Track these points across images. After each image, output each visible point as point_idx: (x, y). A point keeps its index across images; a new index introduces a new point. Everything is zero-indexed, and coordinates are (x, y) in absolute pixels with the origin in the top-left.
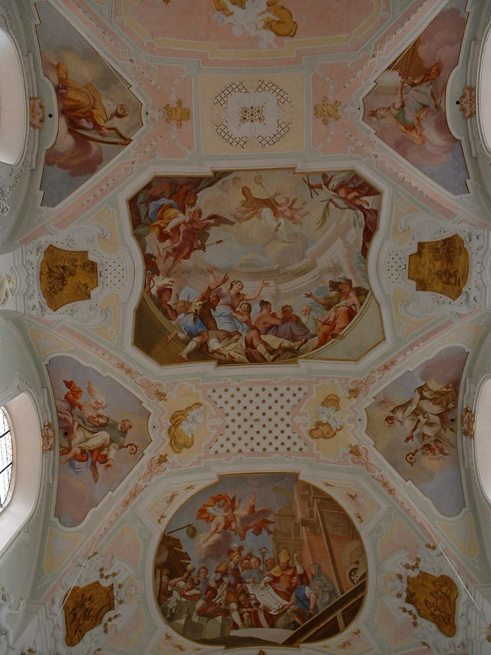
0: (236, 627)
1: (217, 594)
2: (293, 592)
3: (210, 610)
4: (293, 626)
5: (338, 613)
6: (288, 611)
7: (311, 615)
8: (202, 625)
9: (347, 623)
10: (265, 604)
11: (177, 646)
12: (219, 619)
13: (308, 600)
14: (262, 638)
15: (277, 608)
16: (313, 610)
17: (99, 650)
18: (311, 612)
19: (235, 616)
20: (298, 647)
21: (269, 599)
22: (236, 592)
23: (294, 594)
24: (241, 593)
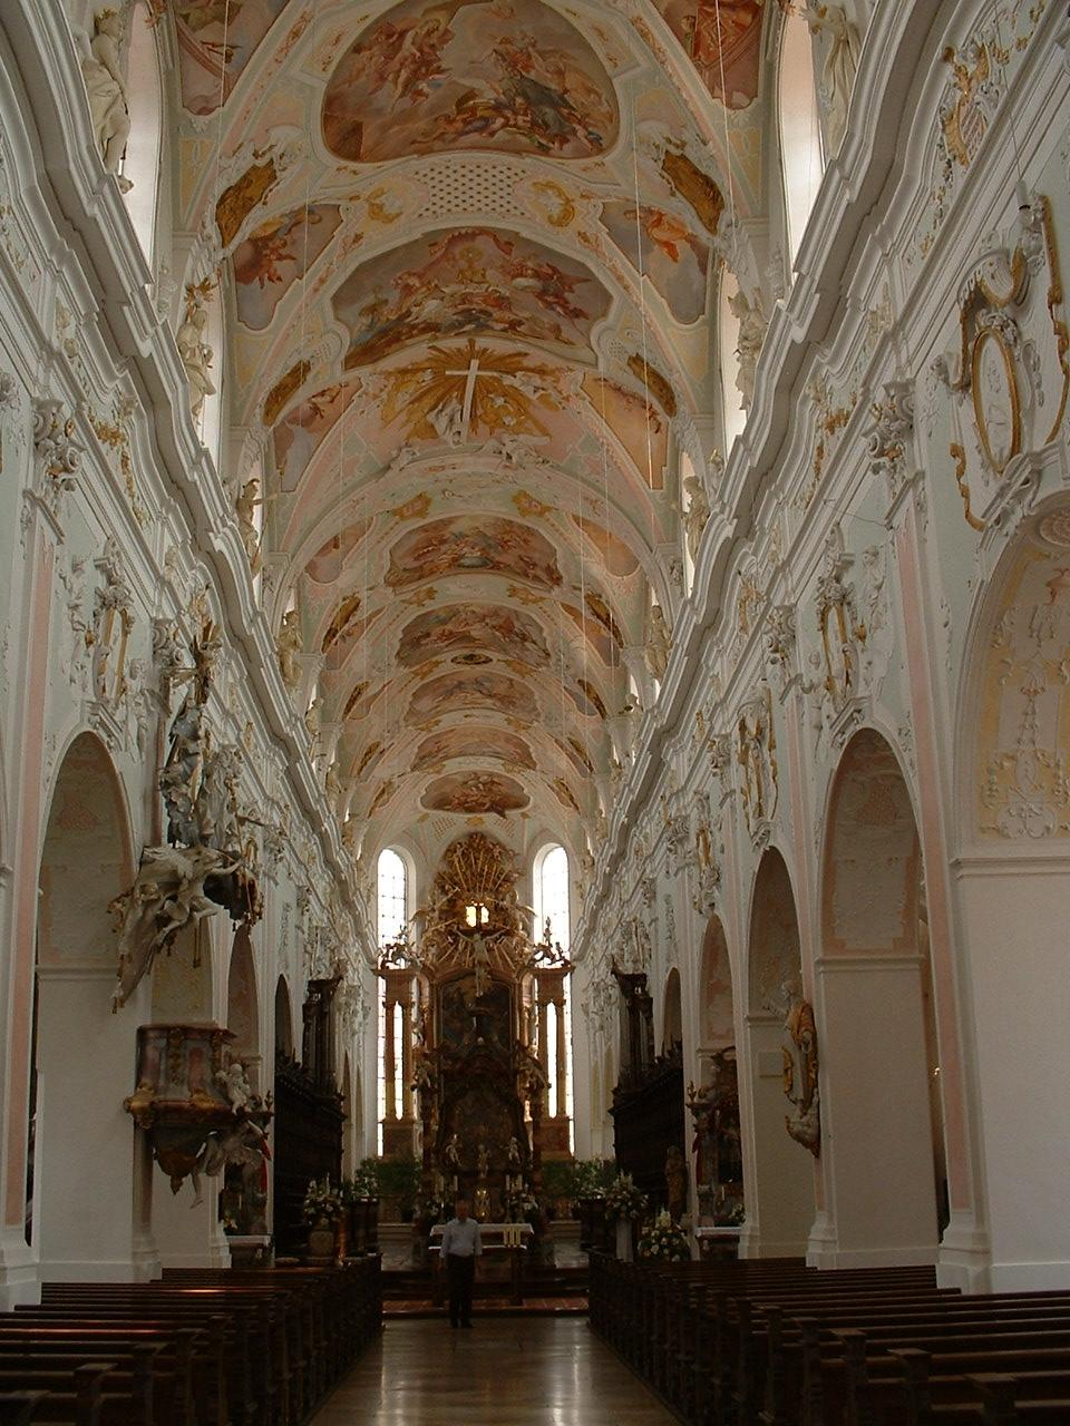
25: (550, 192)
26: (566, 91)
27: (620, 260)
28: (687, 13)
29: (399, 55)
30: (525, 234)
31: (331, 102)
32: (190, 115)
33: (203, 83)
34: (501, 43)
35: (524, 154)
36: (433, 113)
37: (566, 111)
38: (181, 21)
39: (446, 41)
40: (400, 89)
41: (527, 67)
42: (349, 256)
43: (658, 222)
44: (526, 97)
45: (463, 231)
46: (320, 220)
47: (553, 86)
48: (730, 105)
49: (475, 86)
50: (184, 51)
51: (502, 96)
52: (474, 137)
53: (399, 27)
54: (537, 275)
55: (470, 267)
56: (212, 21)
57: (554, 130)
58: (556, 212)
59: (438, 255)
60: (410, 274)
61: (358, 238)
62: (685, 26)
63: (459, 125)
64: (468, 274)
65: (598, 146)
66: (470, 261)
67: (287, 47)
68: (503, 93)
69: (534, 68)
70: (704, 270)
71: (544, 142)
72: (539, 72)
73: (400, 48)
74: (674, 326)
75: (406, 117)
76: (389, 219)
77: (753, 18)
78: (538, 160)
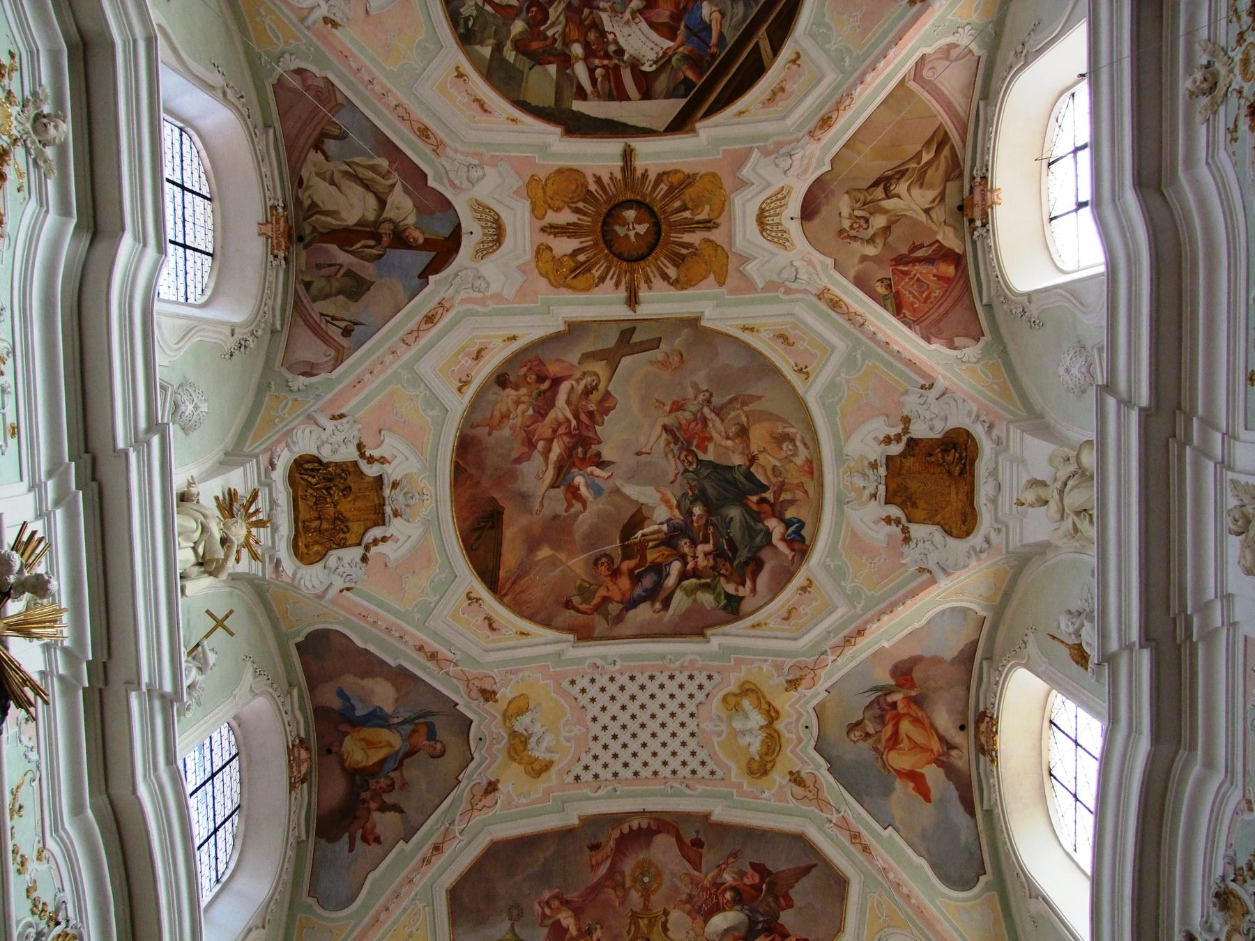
0: (581, 94)
1: (548, 18)
2: (681, 19)
3: (535, 45)
4: (682, 91)
5: (762, 34)
6: (674, 59)
7: (714, 56)
8: (522, 72)
9: (776, 50)
10: (632, 52)
11: (476, 100)
12: (552, 69)
13: (708, 28)
14: (631, 122)
15: (653, 56)
16: (717, 45)
17: (335, 25)
18: (714, 50)
19: (580, 70)
20: (693, 131)
21: (640, 42)
22: (582, 22)
23: (683, 24)
24: (589, 30)
25: (746, 703)
26: (753, 460)
27: (854, 810)
28: (881, 274)
29: (552, 415)
30: (720, 813)
31: (466, 447)
32: (289, 375)
33: (310, 349)
34: (671, 411)
35: (709, 632)
36: (593, 546)
37: (754, 498)
38: (301, 289)
39: (607, 411)
40: (551, 473)
41: (705, 440)
42: (478, 818)
43: (895, 739)
44: (701, 497)
45: (635, 825)
46: (443, 753)
47: (737, 460)
48: (951, 346)
49: (643, 500)
50: (299, 319)
51: (677, 512)
52: (644, 612)
53: (554, 369)
54: (740, 898)
55: (646, 908)
56: (336, 294)
57: (744, 554)
58: (755, 745)
59: (603, 870)
60: (566, 903)
61: (492, 787)
62: (881, 289)
63: (625, 582)
64: (643, 923)
65: (800, 544)
66: (646, 893)
67: (418, 330)
68: (678, 506)
69: (710, 439)
70: (968, 806)
71: (730, 588)
72: (721, 449)
73: (551, 404)
74: (943, 895)
75: (555, 531)
76: (539, 769)
77: (956, 268)
78: (724, 635)
